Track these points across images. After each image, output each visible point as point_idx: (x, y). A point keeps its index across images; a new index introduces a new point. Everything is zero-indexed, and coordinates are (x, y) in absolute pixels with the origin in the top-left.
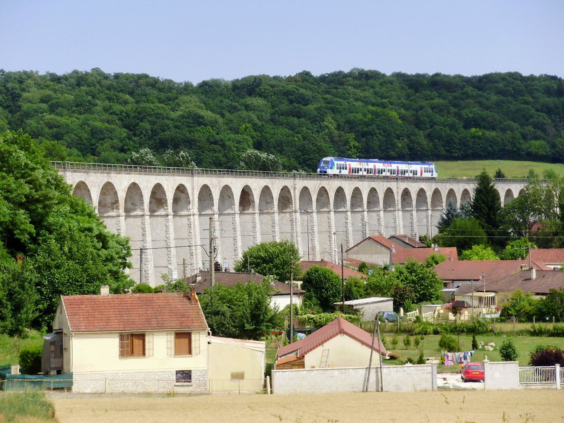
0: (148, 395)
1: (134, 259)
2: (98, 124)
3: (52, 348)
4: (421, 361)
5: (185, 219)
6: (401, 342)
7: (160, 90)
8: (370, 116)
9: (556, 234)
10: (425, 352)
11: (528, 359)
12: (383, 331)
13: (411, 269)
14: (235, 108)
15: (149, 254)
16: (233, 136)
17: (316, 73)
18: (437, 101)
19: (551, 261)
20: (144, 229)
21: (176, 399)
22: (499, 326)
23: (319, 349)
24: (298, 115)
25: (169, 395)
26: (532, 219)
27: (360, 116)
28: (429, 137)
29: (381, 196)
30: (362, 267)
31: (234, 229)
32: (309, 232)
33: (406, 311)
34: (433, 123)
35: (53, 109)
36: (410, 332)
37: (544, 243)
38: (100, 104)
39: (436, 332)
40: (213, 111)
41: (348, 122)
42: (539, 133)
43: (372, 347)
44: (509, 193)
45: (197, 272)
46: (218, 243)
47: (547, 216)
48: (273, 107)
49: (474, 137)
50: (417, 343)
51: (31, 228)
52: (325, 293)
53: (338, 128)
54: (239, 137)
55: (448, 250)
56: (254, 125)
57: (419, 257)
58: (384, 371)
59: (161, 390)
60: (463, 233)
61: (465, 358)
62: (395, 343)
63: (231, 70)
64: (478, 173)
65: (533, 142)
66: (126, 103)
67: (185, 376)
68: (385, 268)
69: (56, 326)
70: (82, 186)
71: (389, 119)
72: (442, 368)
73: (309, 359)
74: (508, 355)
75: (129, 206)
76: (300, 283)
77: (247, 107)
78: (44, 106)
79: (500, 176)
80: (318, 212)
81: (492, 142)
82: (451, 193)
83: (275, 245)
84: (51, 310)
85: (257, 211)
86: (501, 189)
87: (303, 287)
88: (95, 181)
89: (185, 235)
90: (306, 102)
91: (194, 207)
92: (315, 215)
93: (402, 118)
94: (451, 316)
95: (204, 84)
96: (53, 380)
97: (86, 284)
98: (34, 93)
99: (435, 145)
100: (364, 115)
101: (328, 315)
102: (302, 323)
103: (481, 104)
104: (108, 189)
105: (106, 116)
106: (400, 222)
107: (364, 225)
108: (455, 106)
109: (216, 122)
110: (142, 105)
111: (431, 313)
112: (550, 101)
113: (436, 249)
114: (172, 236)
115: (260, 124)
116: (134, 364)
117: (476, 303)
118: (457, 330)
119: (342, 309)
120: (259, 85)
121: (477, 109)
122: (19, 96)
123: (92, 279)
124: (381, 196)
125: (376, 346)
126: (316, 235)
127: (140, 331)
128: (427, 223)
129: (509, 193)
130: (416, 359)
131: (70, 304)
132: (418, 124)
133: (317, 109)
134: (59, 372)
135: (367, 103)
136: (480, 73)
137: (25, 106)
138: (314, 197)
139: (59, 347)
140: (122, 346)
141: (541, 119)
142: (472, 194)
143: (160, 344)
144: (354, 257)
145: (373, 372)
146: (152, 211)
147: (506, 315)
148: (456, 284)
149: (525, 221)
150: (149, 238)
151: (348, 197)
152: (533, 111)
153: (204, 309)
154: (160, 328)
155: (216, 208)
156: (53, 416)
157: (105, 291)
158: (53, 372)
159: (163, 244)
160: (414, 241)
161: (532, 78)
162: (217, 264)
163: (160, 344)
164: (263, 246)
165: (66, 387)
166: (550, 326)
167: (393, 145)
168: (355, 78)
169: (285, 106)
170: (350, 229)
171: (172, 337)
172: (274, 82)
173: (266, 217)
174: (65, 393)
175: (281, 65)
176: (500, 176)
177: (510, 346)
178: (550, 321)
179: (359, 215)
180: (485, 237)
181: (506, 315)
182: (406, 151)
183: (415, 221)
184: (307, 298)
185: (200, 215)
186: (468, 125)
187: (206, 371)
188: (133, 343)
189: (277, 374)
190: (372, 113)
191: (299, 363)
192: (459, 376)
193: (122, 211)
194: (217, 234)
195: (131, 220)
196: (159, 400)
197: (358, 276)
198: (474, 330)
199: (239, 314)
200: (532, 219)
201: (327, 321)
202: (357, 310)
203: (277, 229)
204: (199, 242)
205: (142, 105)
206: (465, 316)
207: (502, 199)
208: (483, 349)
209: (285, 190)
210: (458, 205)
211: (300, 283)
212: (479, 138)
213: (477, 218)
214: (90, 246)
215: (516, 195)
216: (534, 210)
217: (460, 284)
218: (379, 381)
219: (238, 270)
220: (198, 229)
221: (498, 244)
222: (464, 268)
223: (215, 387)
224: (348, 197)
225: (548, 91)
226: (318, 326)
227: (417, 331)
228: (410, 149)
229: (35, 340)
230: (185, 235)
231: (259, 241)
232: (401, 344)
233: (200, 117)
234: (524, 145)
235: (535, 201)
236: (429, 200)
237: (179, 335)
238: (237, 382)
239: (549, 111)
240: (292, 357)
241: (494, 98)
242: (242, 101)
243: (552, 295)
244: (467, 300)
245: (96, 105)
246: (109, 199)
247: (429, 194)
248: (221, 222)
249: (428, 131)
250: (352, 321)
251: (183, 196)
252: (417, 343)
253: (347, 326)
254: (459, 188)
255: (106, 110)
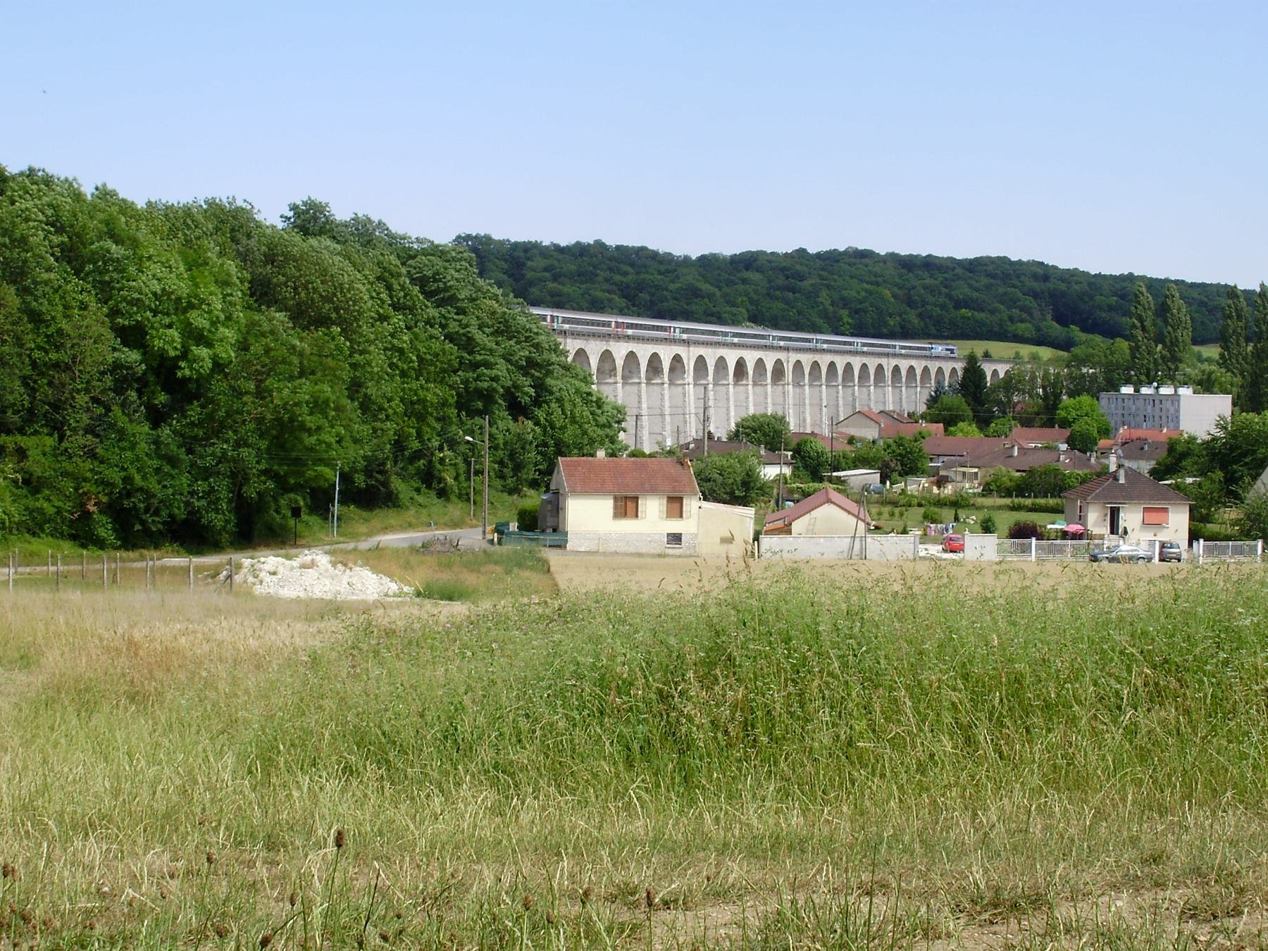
0: (640, 555)
1: (629, 424)
2: (599, 294)
3: (549, 507)
4: (905, 532)
5: (680, 388)
6: (886, 512)
7: (661, 262)
8: (863, 294)
9: (1038, 414)
10: (909, 523)
11: (1006, 532)
12: (868, 503)
13: (899, 444)
14: (732, 281)
15: (645, 420)
16: (728, 309)
17: (812, 250)
18: (929, 281)
19: (1032, 440)
20: (640, 397)
21: (667, 560)
22: (980, 501)
23: (806, 518)
24: (794, 291)
25: (660, 556)
26: (1015, 399)
27: (853, 293)
28: (920, 316)
29: (872, 372)
30: (851, 441)
31: (728, 399)
32: (800, 404)
33: (892, 484)
34: (924, 303)
35: (555, 278)
36: (895, 504)
37: (1027, 422)
38: (602, 274)
39: (920, 505)
40: (711, 284)
41: (843, 299)
42: (1024, 315)
43: (857, 517)
44: (995, 372)
45: (690, 439)
46: (711, 412)
47: (1031, 396)
48: (770, 282)
49: (964, 317)
50: (901, 515)
51: (532, 391)
52: (814, 467)
53: (833, 304)
54: (734, 310)
55: (935, 425)
56: (750, 299)
57: (908, 431)
58: (869, 540)
59: (653, 551)
60: (949, 409)
61: (947, 530)
62: (880, 514)
63: (729, 245)
64: (967, 353)
65: (1019, 324)
66: (626, 274)
67: (676, 538)
68: (874, 442)
69: (553, 487)
70: (581, 353)
71: (883, 299)
72: (925, 538)
73: (797, 526)
74: (987, 528)
75: (627, 373)
76: (790, 453)
77: (744, 281)
78: (547, 274)
79: (987, 356)
80: (810, 385)
81: (981, 323)
82: (940, 370)
83: (765, 415)
84: (550, 471)
85: (751, 382)
86: (988, 368)
87: (793, 457)
88: (594, 350)
89: (680, 404)
90: (802, 278)
91: (689, 377)
92: (807, 388)
93: (895, 296)
94: (935, 490)
95: (702, 258)
96: (550, 538)
97: (584, 448)
98: (540, 263)
99: (926, 324)
100: (858, 293)
101: (816, 485)
102: (791, 491)
103: (971, 287)
104: (607, 356)
105: (606, 286)
106: (890, 397)
107: (854, 400)
108: (946, 287)
109: (714, 294)
110: (642, 276)
111: (917, 486)
112: (1037, 286)
113: (924, 424)
114: (667, 404)
115: (755, 297)
116: (627, 525)
117: (959, 478)
118: (940, 503)
119: (830, 480)
120: (755, 260)
121: (967, 290)
122: (524, 264)
123: (592, 442)
124: (872, 372)
125: (861, 516)
126: (808, 407)
127: (633, 494)
128: (915, 400)
129: (995, 372)
130: (901, 529)
131: (567, 465)
132: (910, 303)
133: (812, 285)
134: (555, 530)
135: (862, 281)
136: (971, 255)
137: (530, 275)
138: (807, 371)
139: (556, 507)
140: (616, 507)
141: (1027, 303)
142: (960, 373)
143: (653, 507)
144: (845, 430)
145: (857, 541)
146: (649, 379)
147: (987, 491)
148: (941, 459)
149: (1010, 401)
150: (644, 406)
151: (840, 372)
152: (1020, 295)
153: (698, 475)
154: (653, 491)
155: (710, 378)
156: (549, 571)
157: (601, 454)
158: (549, 530)
159: (659, 412)
160: (902, 416)
161: (1020, 262)
162: (709, 433)
163: (653, 507)
164: (754, 417)
165: (561, 546)
166: (1028, 502)
167: (886, 324)
168: (850, 257)
169: (780, 281)
170: (841, 402)
171: (665, 501)
172: (770, 258)
173: (759, 389)
174: (559, 551)
175: (779, 242)
176: (987, 356)
177: (989, 520)
178: (1029, 497)
179: (850, 390)
180: (970, 414)
181: (987, 491)
182: (898, 329)
183: (904, 396)
184: (796, 468)
185: (695, 385)
186: (958, 305)
187: (696, 535)
188: (626, 506)
189: (766, 541)
190: (866, 291)
191: (787, 530)
192: (940, 547)
193: (619, 378)
194: (711, 403)
195: (628, 388)
196: (650, 560)
197: (848, 448)
198: (957, 503)
199: (731, 481)
200: (1015, 399)
201: (815, 491)
202: (845, 481)
203: (769, 400)
204: (693, 411)
205: (642, 276)
206: (949, 490)
207: (988, 379)
208: (965, 522)
209: (779, 363)
210: (946, 383)
211: (790, 453)
212: (968, 318)
213: (964, 396)
214: (583, 411)
215: (1002, 375)
216: (1019, 390)
217: (945, 459)
218: (863, 550)
219: (730, 439)
220: (692, 397)
221: (983, 422)
222: (948, 443)
223: (704, 550)
224: (840, 372)
225: (1035, 277)
226: (806, 495)
227: (902, 502)
228: (902, 327)
229: (533, 499)
230: (680, 404)
231: (751, 411)
232: (886, 515)
233: (698, 289)
234: (1011, 328)
235: (1020, 382)
236: (918, 377)
237: (671, 499)
238: (725, 547)
239: (1036, 295)
240: (780, 524)
241: (985, 280)
242: (739, 275)
243: (1031, 472)
244: (951, 474)
245: (597, 275)
246: (607, 367)
247: (919, 372)
248: (715, 392)
249: (919, 310)
250: (839, 491)
251: (679, 365)
252: (901, 515)
253: (834, 495)
254: (947, 367)
255: (607, 280)
